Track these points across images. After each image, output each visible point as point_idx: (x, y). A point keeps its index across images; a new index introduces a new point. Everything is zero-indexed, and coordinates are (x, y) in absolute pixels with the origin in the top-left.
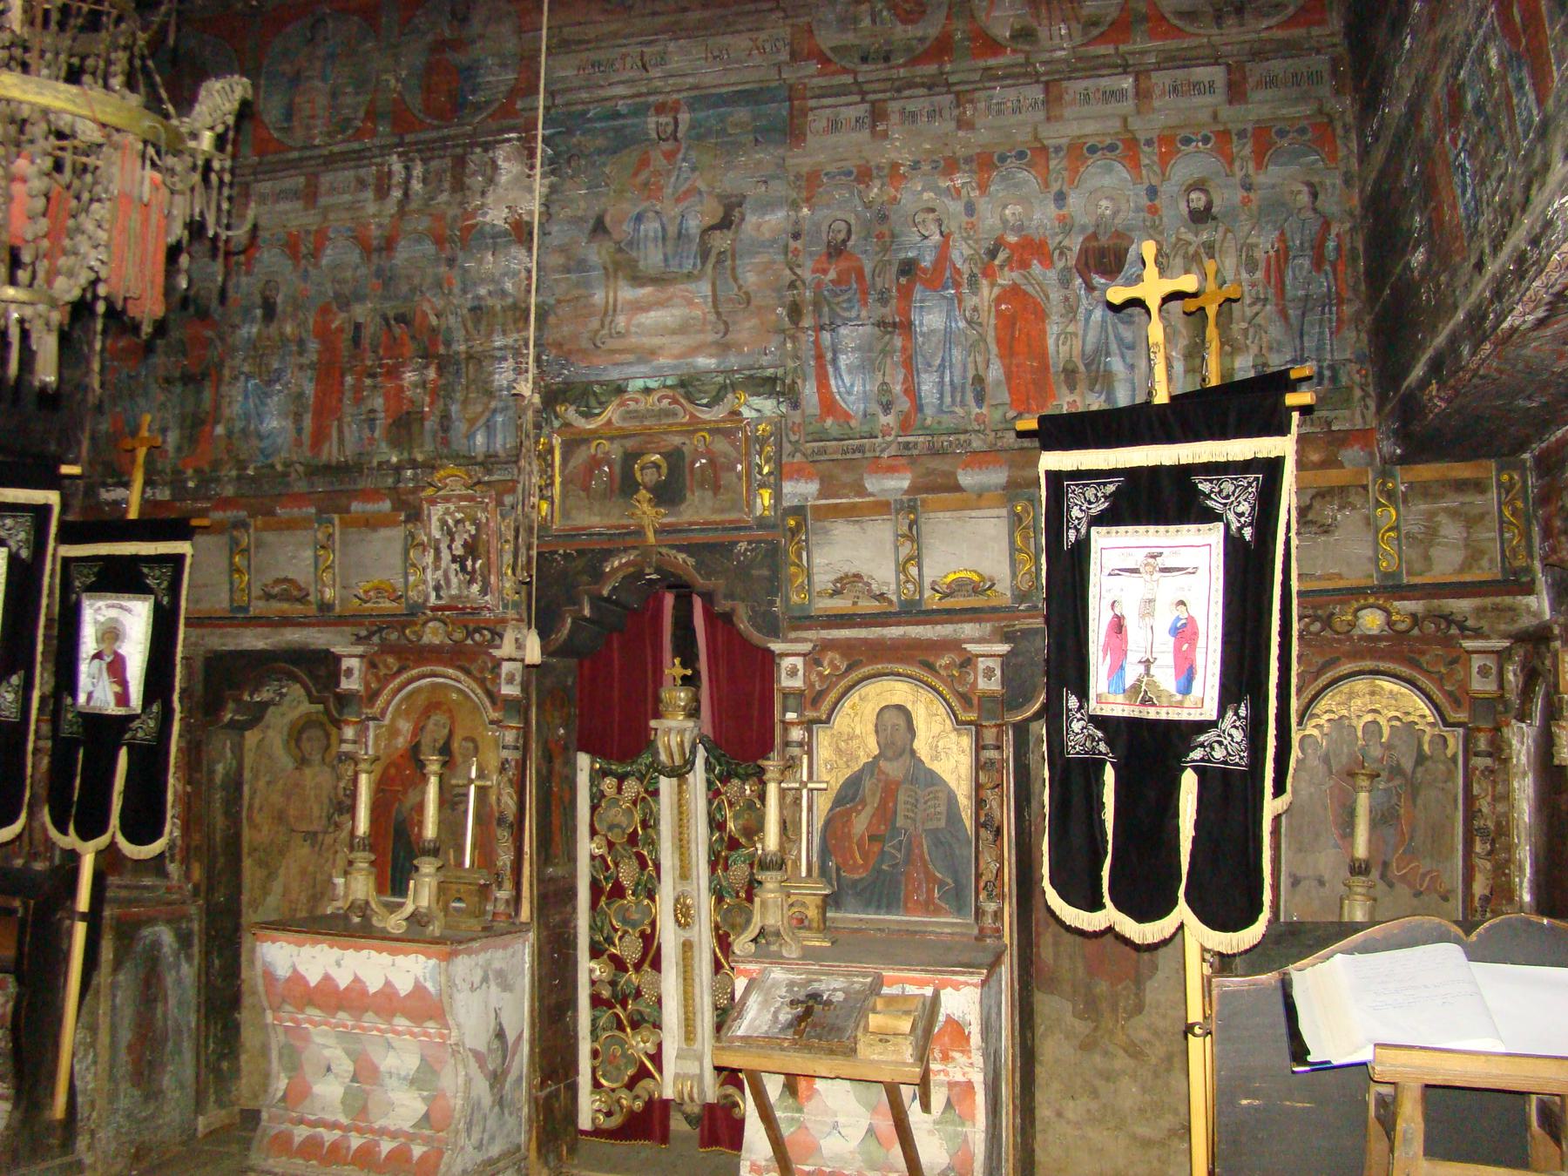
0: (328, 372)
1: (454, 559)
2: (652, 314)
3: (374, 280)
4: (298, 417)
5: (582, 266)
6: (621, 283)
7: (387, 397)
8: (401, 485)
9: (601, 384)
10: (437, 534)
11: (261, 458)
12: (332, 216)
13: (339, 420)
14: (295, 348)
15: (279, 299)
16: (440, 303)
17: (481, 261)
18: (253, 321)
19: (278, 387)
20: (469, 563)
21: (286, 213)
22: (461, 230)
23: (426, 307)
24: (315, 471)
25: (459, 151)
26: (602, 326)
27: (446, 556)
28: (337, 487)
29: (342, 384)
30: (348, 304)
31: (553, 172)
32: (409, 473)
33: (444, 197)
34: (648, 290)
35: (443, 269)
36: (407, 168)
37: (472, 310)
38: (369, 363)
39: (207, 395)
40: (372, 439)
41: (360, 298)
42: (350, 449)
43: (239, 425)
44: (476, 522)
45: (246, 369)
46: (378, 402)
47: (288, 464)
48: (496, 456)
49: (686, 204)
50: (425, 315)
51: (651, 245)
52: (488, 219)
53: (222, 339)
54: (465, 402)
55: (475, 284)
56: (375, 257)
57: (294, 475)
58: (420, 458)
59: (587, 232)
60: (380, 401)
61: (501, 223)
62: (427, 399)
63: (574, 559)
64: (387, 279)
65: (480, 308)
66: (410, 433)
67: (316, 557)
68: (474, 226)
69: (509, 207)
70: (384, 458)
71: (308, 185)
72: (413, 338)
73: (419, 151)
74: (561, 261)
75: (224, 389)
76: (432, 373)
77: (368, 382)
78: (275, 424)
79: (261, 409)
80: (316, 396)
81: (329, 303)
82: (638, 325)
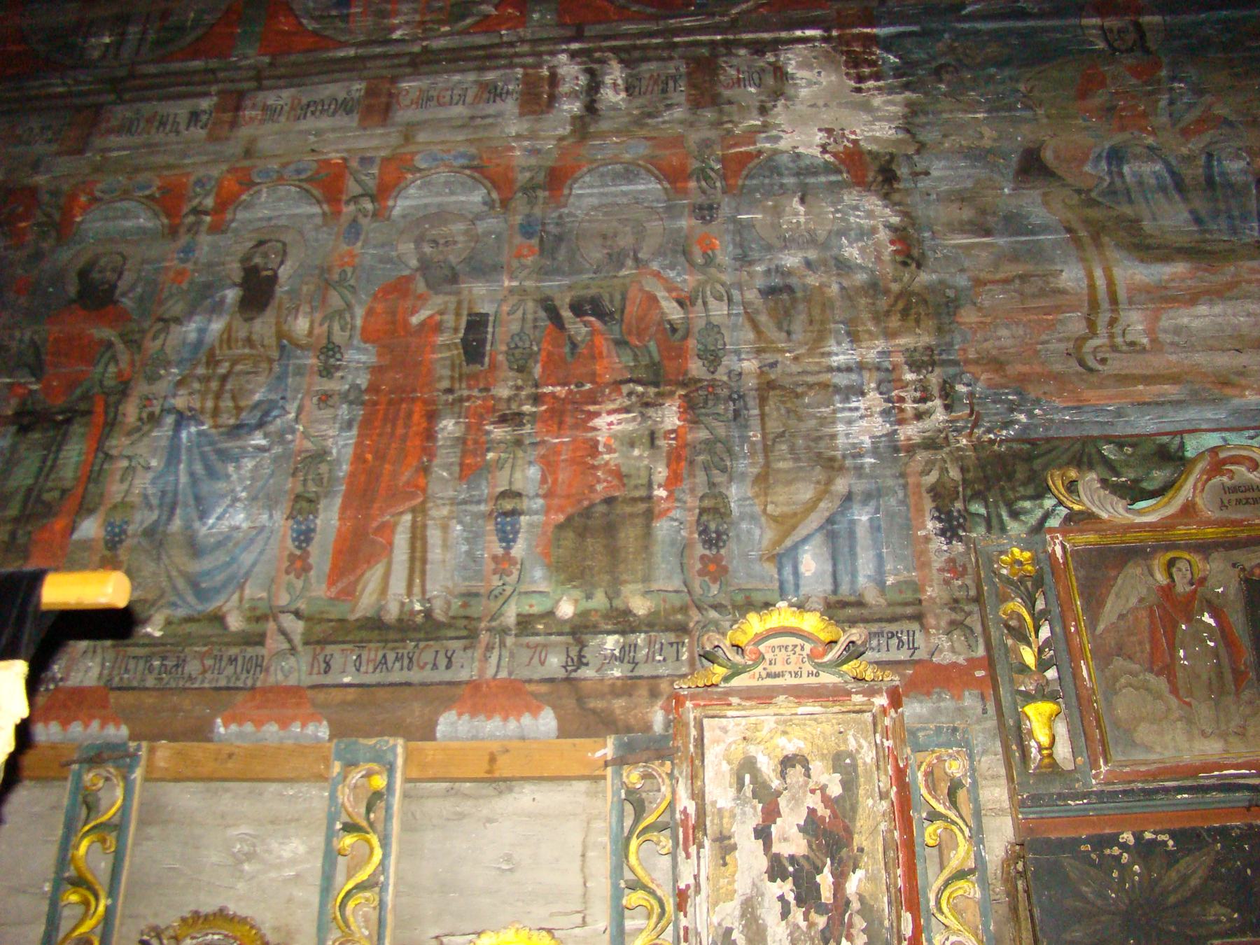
0: (395, 410)
1: (776, 870)
2: (1202, 309)
3: (518, 240)
4: (304, 505)
5: (1014, 223)
6: (1113, 254)
7: (549, 464)
8: (588, 673)
9: (1120, 443)
10: (720, 793)
11: (191, 599)
12: (422, 137)
13: (420, 511)
14: (312, 361)
15: (284, 272)
16: (687, 280)
17: (777, 211)
18: (217, 308)
19: (258, 440)
20: (825, 880)
21: (319, 133)
22: (723, 160)
23: (651, 285)
24: (328, 633)
25: (705, 51)
26: (1091, 325)
27: (750, 858)
28: (396, 676)
29: (430, 435)
30: (454, 278)
31: (907, 87)
32: (611, 642)
33: (678, 113)
34: (1179, 268)
35: (685, 223)
36: (591, 72)
37: (770, 292)
38: (504, 392)
39: (74, 453)
40: (503, 563)
41: (483, 269)
42: (441, 587)
43: (143, 519)
44: (843, 763)
45: (180, 402)
46: (528, 476)
47: (259, 616)
48: (860, 604)
49: (1207, 137)
50: (653, 300)
51: (1160, 196)
52: (783, 145)
53: (134, 344)
54: (763, 479)
55: (769, 248)
56: (519, 203)
57: (275, 643)
58: (641, 607)
59: (1010, 173)
60: (534, 472)
61: (816, 152)
62: (661, 473)
63: (1171, 859)
64: (553, 244)
65: (789, 289)
66: (613, 552)
67: (331, 855)
68: (749, 156)
69: (829, 131)
70: (537, 606)
71: (370, 92)
72: (620, 343)
73: (613, 50)
74: (967, 214)
75: (117, 444)
76: (670, 417)
77: (499, 433)
78: (239, 518)
79: (205, 488)
80: (358, 458)
81: (409, 279)
82: (1177, 331)
